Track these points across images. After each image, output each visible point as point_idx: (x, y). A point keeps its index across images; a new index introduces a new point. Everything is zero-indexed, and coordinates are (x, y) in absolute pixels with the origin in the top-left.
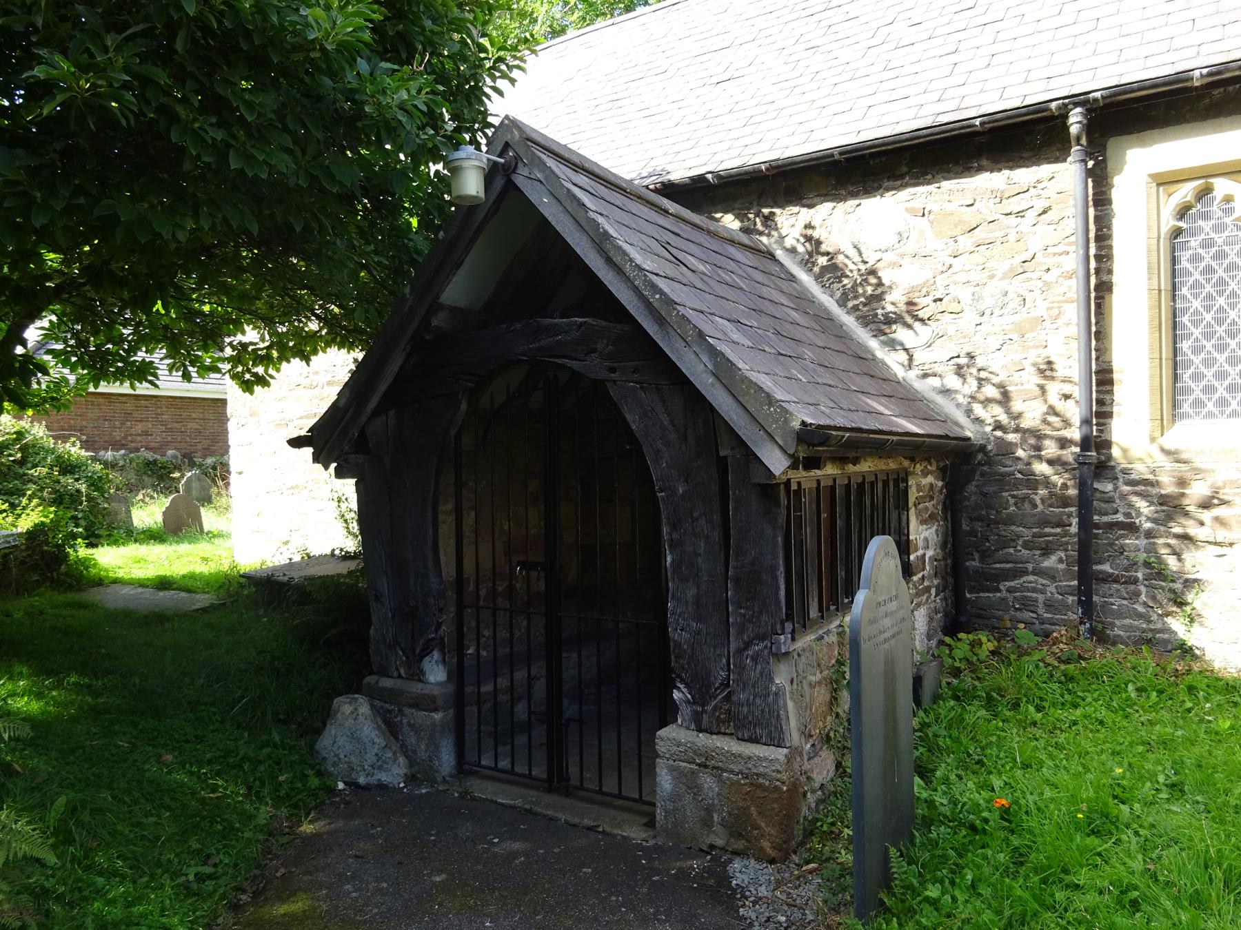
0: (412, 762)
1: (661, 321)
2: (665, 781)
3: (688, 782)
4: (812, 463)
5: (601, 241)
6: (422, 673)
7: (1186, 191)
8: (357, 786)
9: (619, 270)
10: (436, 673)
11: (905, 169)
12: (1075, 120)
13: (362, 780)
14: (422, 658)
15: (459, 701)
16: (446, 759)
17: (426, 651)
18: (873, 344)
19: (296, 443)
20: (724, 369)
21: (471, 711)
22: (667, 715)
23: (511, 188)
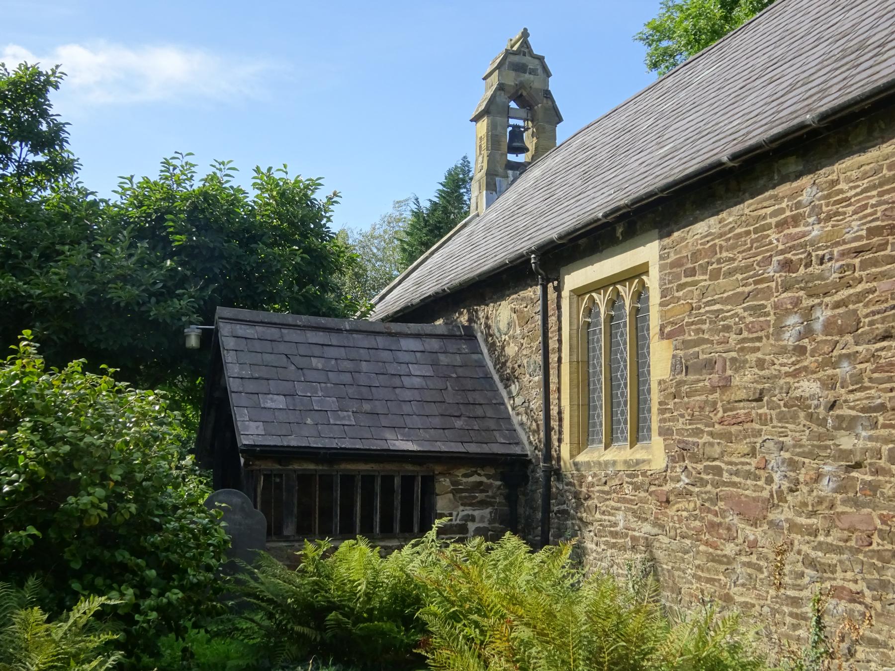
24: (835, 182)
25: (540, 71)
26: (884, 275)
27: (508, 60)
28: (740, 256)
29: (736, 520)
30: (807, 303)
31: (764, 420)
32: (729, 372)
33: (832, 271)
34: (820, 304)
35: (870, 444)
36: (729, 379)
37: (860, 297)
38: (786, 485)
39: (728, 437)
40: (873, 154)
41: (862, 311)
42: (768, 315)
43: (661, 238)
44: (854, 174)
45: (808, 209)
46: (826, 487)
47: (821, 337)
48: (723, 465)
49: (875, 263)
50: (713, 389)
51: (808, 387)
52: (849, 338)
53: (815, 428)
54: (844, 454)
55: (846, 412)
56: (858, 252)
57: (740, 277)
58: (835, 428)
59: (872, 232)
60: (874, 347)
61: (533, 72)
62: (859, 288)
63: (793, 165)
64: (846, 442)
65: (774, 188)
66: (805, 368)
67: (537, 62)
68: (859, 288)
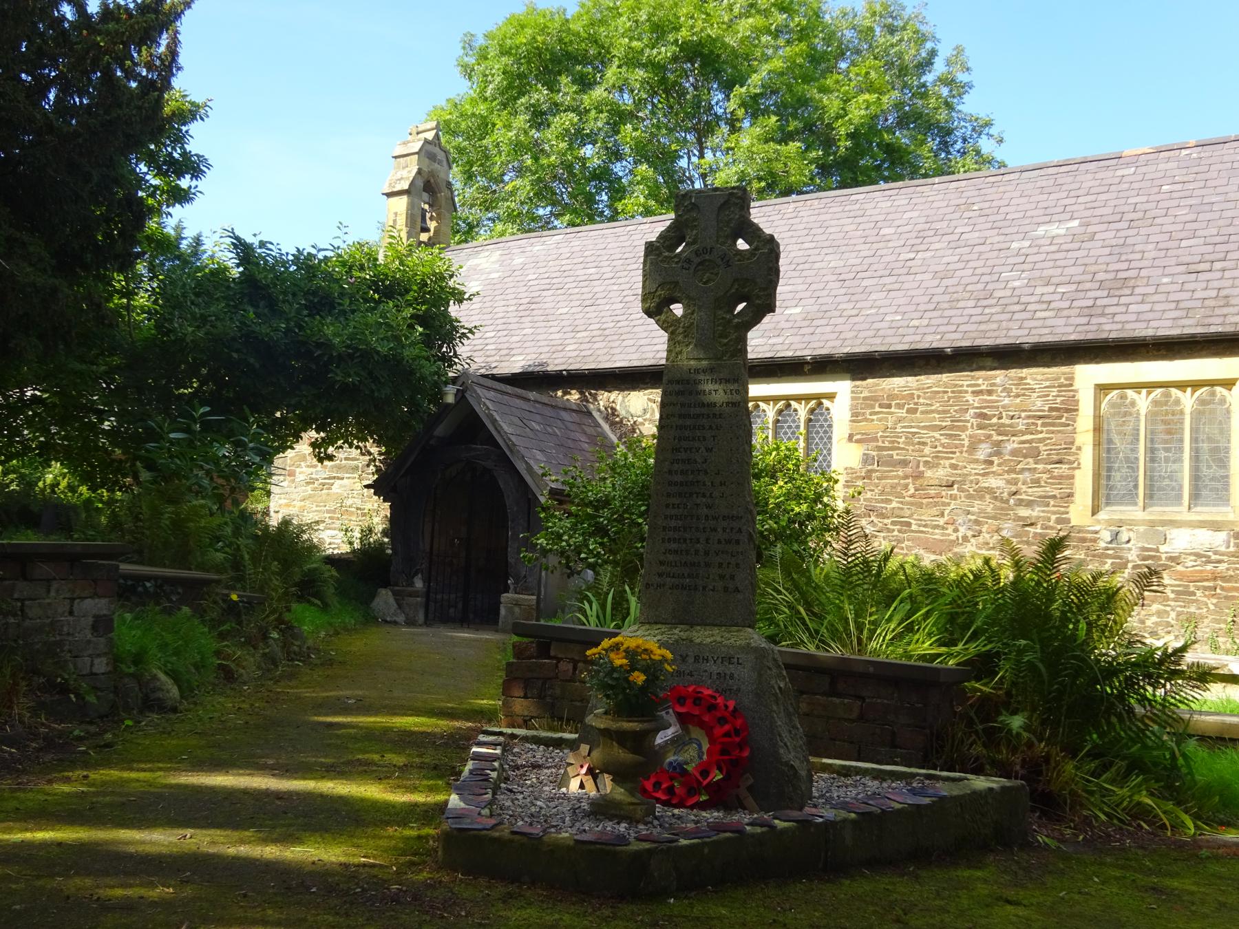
0: (407, 619)
1: (511, 451)
2: (503, 611)
3: (510, 611)
5: (494, 421)
6: (413, 583)
8: (386, 622)
9: (499, 432)
10: (419, 584)
11: (648, 380)
13: (388, 619)
14: (413, 577)
15: (427, 595)
16: (421, 617)
17: (416, 574)
19: (367, 487)
21: (432, 605)
23: (463, 397)
24: (1022, 378)
25: (445, 163)
26: (1059, 432)
27: (426, 147)
28: (938, 405)
29: (922, 552)
30: (996, 438)
31: (953, 498)
32: (922, 468)
33: (1021, 425)
34: (1009, 440)
35: (1042, 514)
36: (923, 472)
37: (1041, 441)
38: (970, 533)
39: (920, 506)
40: (1055, 369)
41: (1042, 447)
42: (963, 440)
43: (853, 380)
44: (1039, 377)
45: (1000, 389)
47: (1007, 457)
48: (912, 521)
49: (1053, 425)
50: (906, 477)
51: (993, 482)
52: (1031, 460)
53: (998, 504)
55: (1024, 497)
56: (1040, 417)
57: (937, 416)
58: (1015, 505)
59: (1051, 409)
60: (1049, 467)
61: (440, 163)
62: (1040, 436)
63: (989, 362)
64: (1024, 512)
65: (972, 371)
66: (993, 472)
67: (443, 154)
68: (1040, 436)
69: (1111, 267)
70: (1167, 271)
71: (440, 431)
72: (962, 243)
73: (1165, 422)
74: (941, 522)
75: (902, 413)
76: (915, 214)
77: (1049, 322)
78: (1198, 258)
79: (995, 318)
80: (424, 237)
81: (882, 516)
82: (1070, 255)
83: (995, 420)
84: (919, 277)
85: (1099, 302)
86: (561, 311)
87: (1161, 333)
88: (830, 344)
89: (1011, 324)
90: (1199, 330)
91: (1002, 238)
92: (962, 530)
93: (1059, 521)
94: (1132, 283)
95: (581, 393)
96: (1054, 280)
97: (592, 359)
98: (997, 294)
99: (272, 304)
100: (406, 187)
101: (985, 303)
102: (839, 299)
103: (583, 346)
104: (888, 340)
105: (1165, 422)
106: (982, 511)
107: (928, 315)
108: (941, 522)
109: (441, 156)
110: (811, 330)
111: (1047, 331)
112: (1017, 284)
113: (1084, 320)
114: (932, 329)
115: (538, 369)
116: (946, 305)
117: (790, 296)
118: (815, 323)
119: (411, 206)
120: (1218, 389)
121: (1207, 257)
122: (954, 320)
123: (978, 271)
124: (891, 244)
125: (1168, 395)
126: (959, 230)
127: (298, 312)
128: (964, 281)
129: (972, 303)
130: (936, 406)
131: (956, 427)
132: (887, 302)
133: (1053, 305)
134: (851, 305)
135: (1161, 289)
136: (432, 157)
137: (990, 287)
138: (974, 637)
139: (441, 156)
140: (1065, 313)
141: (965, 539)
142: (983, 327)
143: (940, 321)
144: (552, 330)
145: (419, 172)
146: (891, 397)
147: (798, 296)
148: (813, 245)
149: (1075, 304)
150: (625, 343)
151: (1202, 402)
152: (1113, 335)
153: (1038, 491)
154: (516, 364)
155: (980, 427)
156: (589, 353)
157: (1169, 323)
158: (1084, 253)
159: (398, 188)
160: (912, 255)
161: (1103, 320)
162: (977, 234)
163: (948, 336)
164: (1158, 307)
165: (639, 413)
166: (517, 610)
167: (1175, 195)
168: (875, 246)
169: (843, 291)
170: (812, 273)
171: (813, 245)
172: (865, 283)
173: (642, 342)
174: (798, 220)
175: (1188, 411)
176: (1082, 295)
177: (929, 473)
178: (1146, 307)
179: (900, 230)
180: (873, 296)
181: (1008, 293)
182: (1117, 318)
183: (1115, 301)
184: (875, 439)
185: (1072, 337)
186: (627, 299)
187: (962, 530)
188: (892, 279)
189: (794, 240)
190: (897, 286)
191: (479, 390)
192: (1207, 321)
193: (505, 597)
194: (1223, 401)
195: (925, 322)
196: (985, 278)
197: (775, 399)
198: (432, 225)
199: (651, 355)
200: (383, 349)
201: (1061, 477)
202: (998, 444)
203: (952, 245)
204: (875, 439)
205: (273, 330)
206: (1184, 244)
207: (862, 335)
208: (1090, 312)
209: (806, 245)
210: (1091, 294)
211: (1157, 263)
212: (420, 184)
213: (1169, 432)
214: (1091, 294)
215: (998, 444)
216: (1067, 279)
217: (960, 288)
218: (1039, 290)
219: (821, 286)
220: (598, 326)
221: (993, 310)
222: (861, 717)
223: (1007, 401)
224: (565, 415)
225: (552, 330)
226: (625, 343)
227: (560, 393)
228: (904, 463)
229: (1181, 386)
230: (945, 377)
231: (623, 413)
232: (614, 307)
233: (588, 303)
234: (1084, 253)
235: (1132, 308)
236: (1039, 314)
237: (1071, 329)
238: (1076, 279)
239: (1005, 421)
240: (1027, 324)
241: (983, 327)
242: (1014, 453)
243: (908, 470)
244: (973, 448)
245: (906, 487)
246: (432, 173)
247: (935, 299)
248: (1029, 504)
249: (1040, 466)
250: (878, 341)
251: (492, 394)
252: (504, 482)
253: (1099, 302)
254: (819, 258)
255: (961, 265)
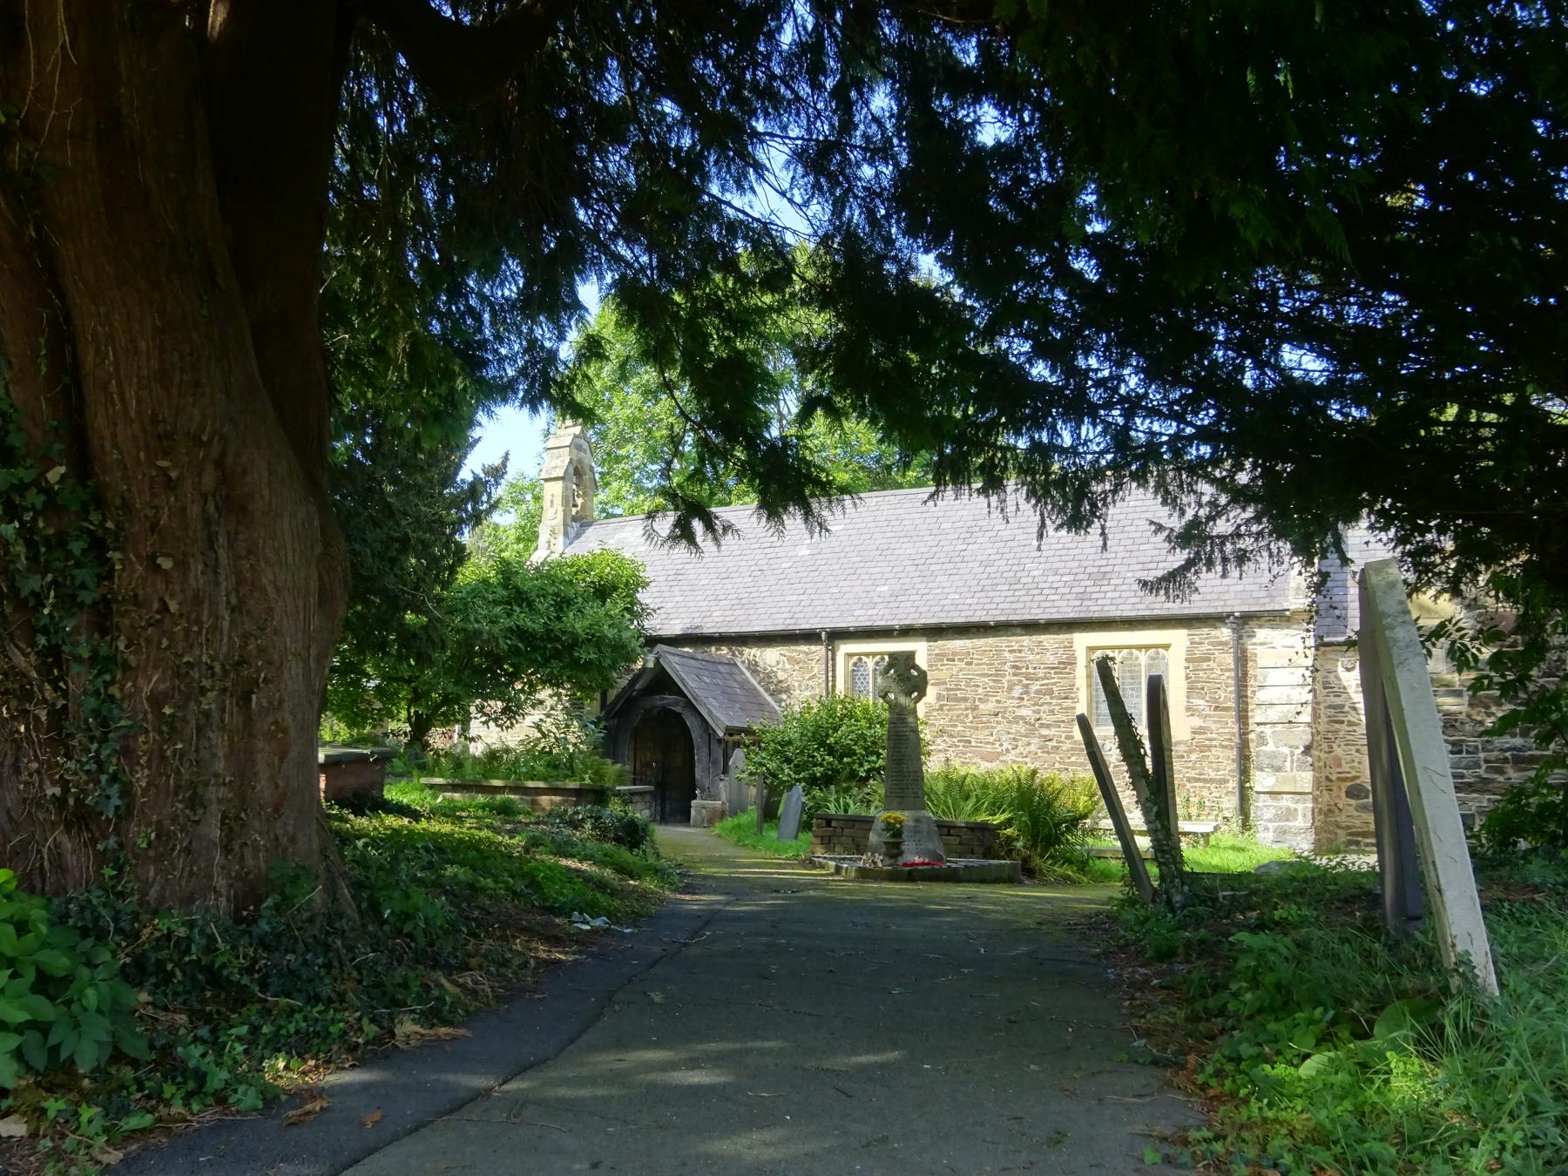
2: (693, 812)
3: (699, 812)
4: (731, 735)
5: (682, 680)
7: (855, 659)
12: (823, 635)
18: (769, 699)
20: (710, 713)
22: (695, 797)
30: (1025, 682)
33: (1041, 673)
37: (1054, 684)
39: (977, 729)
40: (1061, 636)
41: (1055, 688)
46: (1033, 748)
50: (967, 709)
51: (1024, 712)
54: (1042, 736)
61: (585, 451)
63: (1018, 630)
64: (1044, 732)
69: (1097, 563)
70: (1132, 568)
71: (638, 687)
72: (998, 539)
73: (1130, 671)
74: (991, 739)
75: (963, 665)
76: (964, 513)
77: (1057, 604)
78: (1149, 559)
79: (1022, 599)
80: (574, 510)
81: (951, 736)
82: (1071, 552)
83: (1024, 670)
84: (970, 565)
85: (1088, 590)
86: (702, 582)
87: (1125, 614)
88: (911, 616)
89: (1032, 604)
90: (1147, 613)
91: (1025, 536)
92: (1006, 745)
93: (1067, 737)
94: (1109, 576)
95: (730, 649)
96: (1060, 571)
97: (735, 624)
98: (1023, 580)
99: (530, 604)
100: (561, 474)
101: (1015, 587)
102: (915, 580)
103: (727, 613)
104: (951, 614)
105: (1130, 671)
106: (1018, 732)
107: (977, 595)
108: (991, 739)
109: (585, 446)
110: (896, 605)
111: (1054, 610)
112: (1036, 573)
113: (1078, 603)
114: (981, 607)
115: (697, 631)
116: (989, 588)
117: (880, 576)
118: (900, 599)
119: (565, 489)
120: (1160, 650)
121: (1156, 559)
122: (996, 600)
123: (1010, 562)
124: (949, 537)
125: (1131, 654)
126: (996, 528)
127: (547, 609)
128: (1001, 569)
129: (1006, 587)
130: (985, 660)
131: (998, 675)
132: (949, 584)
133: (1059, 591)
134: (924, 585)
135: (1127, 581)
136: (579, 448)
137: (1018, 575)
138: (1004, 811)
139: (585, 446)
140: (1067, 597)
141: (1007, 750)
142: (1014, 606)
143: (985, 600)
144: (698, 598)
145: (571, 461)
146: (955, 654)
147: (886, 576)
148: (892, 534)
149: (1074, 590)
150: (760, 611)
151: (1152, 659)
152: (1096, 615)
153: (1054, 718)
154: (675, 628)
155: (1015, 675)
156: (732, 618)
157: (1129, 607)
158: (1080, 551)
159: (554, 475)
160: (964, 547)
161: (1090, 603)
162: (1008, 532)
163: (991, 612)
164: (1124, 594)
165: (774, 664)
166: (704, 811)
167: (1138, 509)
168: (938, 538)
169: (917, 574)
170: (894, 558)
171: (892, 534)
172: (933, 568)
173: (774, 610)
174: (879, 513)
175: (1143, 664)
176: (1077, 583)
177: (982, 706)
178: (1116, 594)
179: (955, 525)
180: (939, 579)
181: (1030, 580)
182: (1099, 602)
183: (1097, 589)
184: (945, 683)
185: (1072, 615)
186: (755, 574)
187: (1006, 745)
188: (952, 565)
189: (878, 530)
190: (955, 571)
191: (670, 657)
192: (1152, 606)
193: (693, 803)
194: (1164, 658)
195: (975, 601)
196: (1015, 568)
197: (874, 654)
198: (579, 501)
199: (781, 621)
200: (610, 633)
201: (1067, 708)
202: (1027, 686)
203: (993, 540)
204: (945, 683)
205: (534, 624)
206: (1142, 547)
207: (933, 609)
208: (1082, 597)
209: (888, 535)
210: (1083, 583)
211: (1125, 561)
212: (571, 471)
213: (1132, 678)
214: (1083, 583)
215: (1027, 686)
216: (1068, 571)
217: (998, 575)
218: (1051, 579)
219: (901, 569)
220: (735, 596)
221: (1021, 593)
222: (960, 844)
223: (1031, 657)
224: (720, 668)
225: (698, 598)
226: (760, 611)
227: (713, 649)
228: (965, 699)
229: (1139, 648)
230: (990, 640)
231: (761, 664)
232: (745, 580)
233: (723, 576)
234: (1080, 551)
235: (1109, 595)
236: (1050, 598)
237: (1070, 609)
238: (1074, 571)
239: (1031, 670)
240: (1043, 604)
241: (1014, 606)
242: (1037, 692)
243: (968, 704)
244: (1010, 689)
245: (967, 716)
246: (580, 461)
247: (982, 582)
248: (1048, 726)
249: (1054, 701)
250: (944, 614)
251: (677, 658)
252: (691, 722)
253: (1088, 590)
254: (898, 546)
255: (998, 557)
